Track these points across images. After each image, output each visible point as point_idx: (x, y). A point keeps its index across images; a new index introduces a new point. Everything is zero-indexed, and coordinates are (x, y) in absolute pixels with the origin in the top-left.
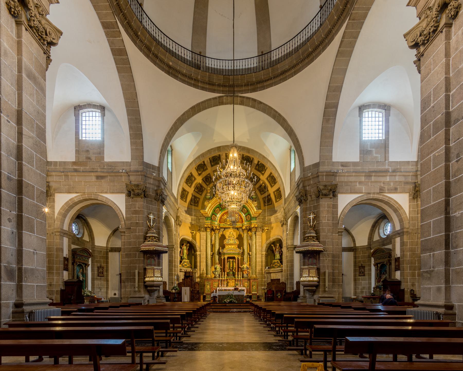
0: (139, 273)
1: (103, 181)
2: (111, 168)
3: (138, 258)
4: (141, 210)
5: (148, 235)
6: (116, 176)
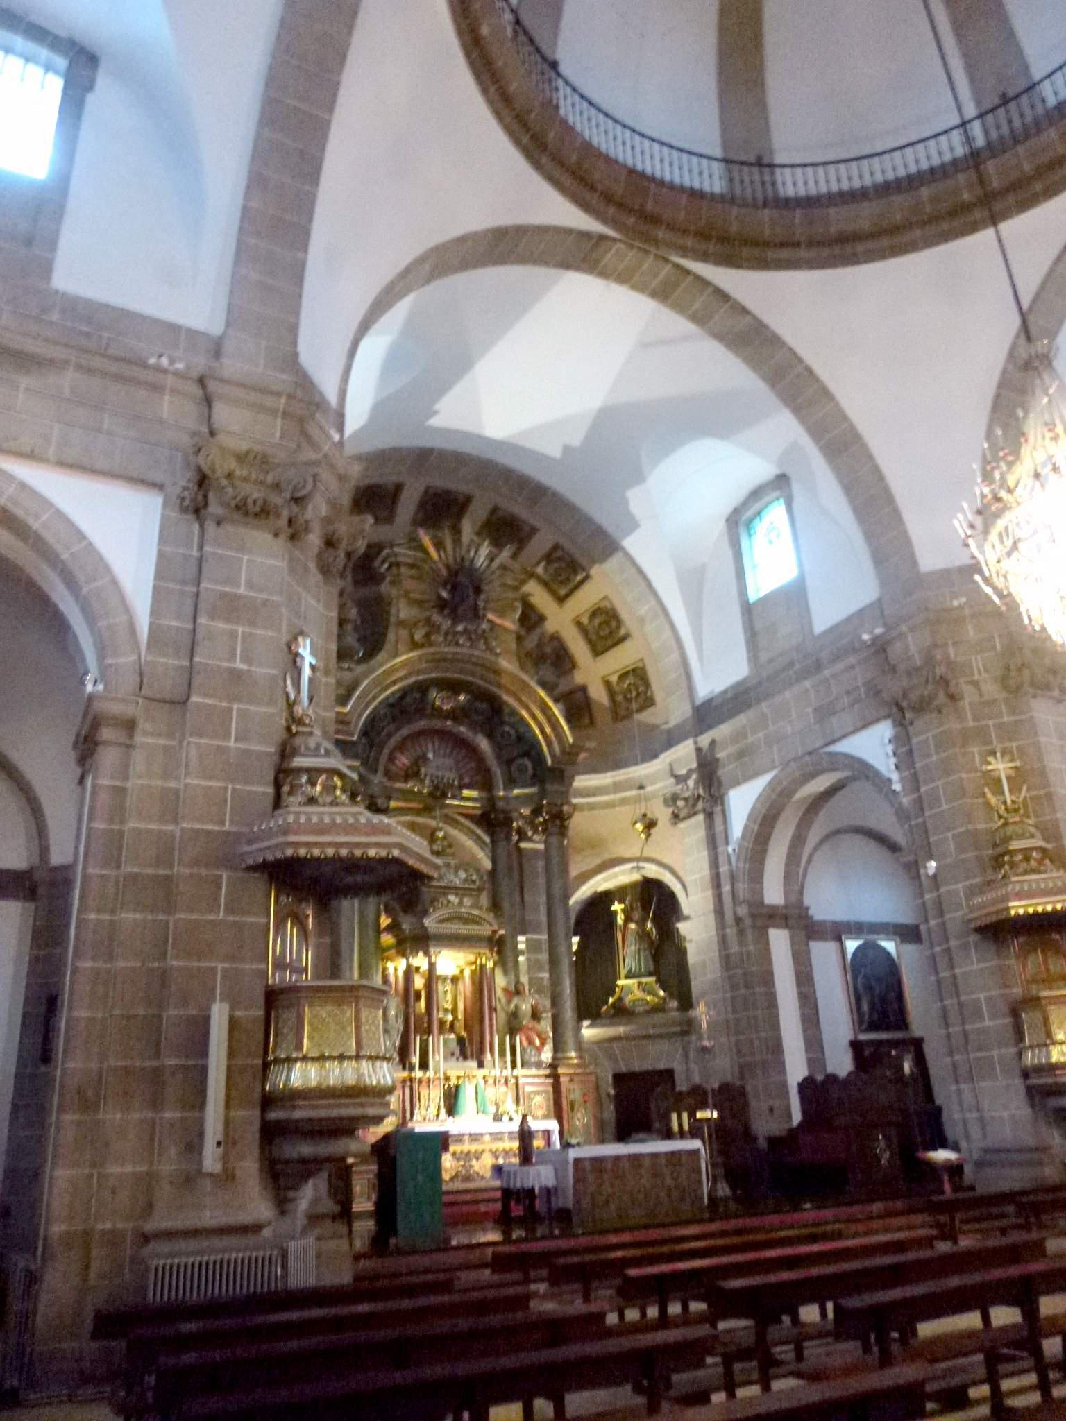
0: (233, 1024)
1: (24, 381)
2: (87, 335)
3: (230, 910)
4: (265, 603)
5: (298, 762)
6: (118, 378)
